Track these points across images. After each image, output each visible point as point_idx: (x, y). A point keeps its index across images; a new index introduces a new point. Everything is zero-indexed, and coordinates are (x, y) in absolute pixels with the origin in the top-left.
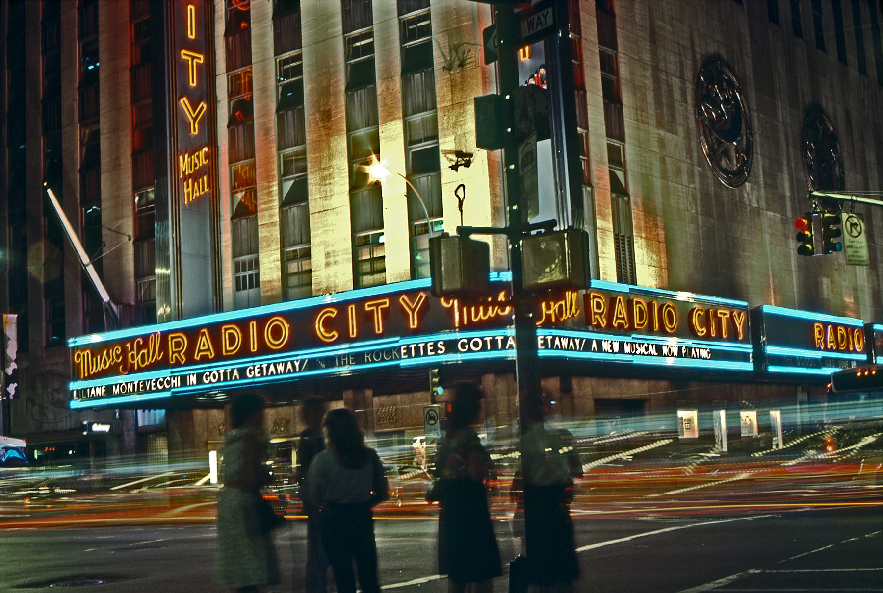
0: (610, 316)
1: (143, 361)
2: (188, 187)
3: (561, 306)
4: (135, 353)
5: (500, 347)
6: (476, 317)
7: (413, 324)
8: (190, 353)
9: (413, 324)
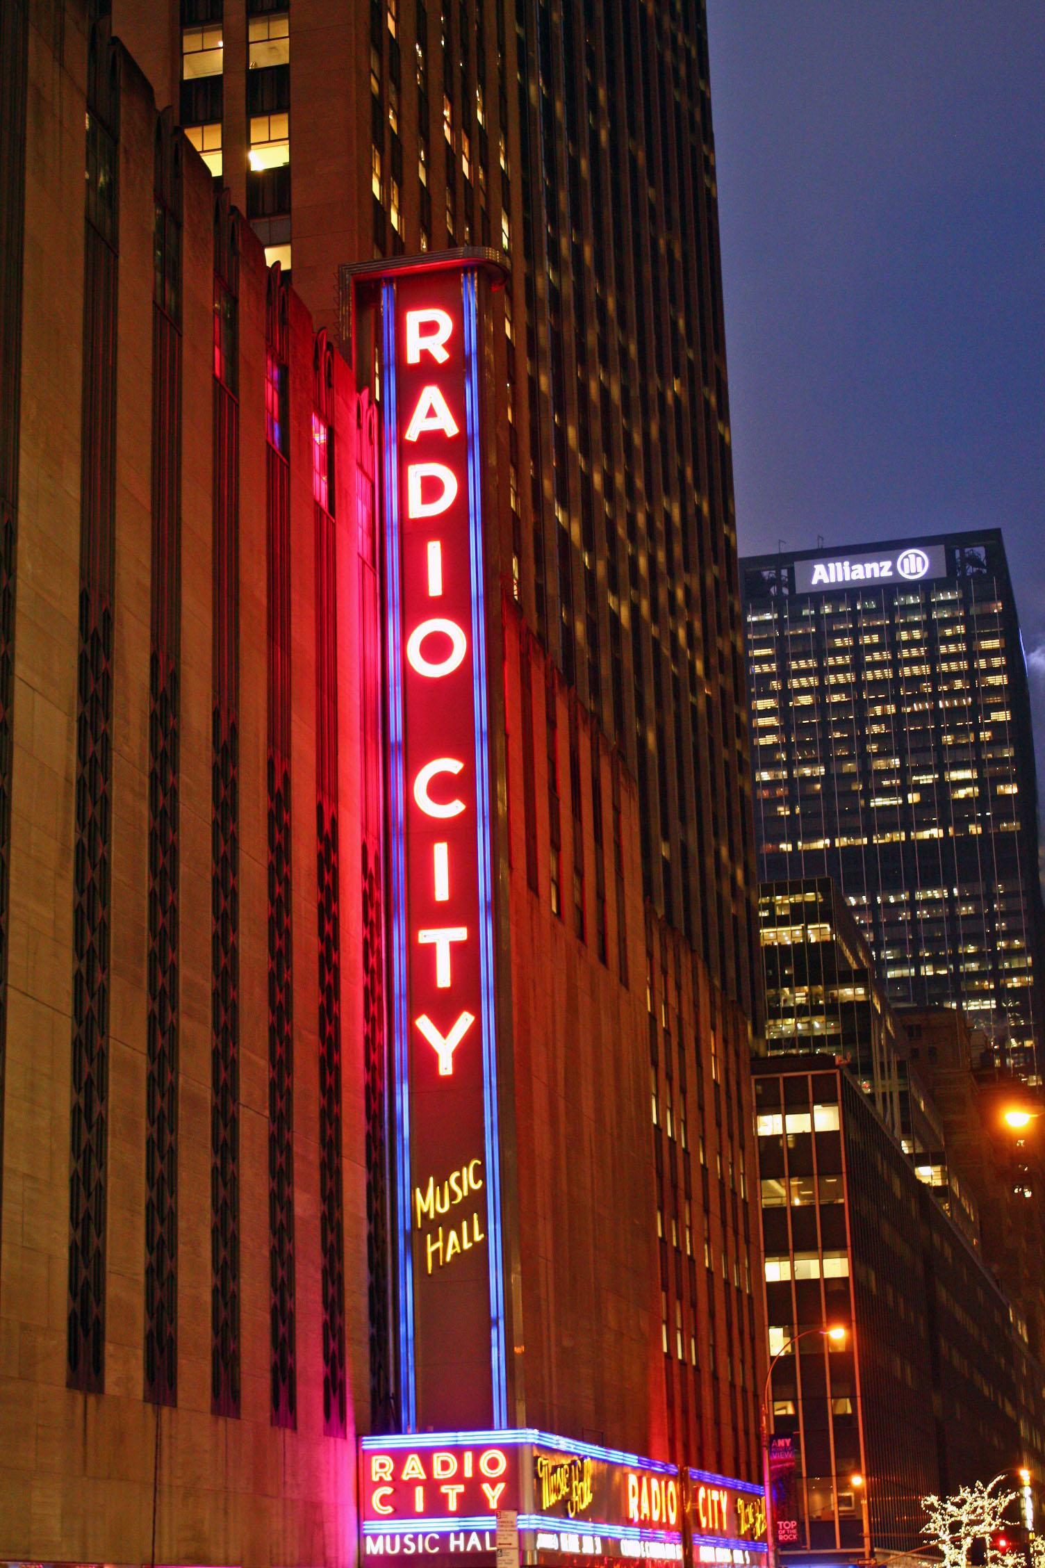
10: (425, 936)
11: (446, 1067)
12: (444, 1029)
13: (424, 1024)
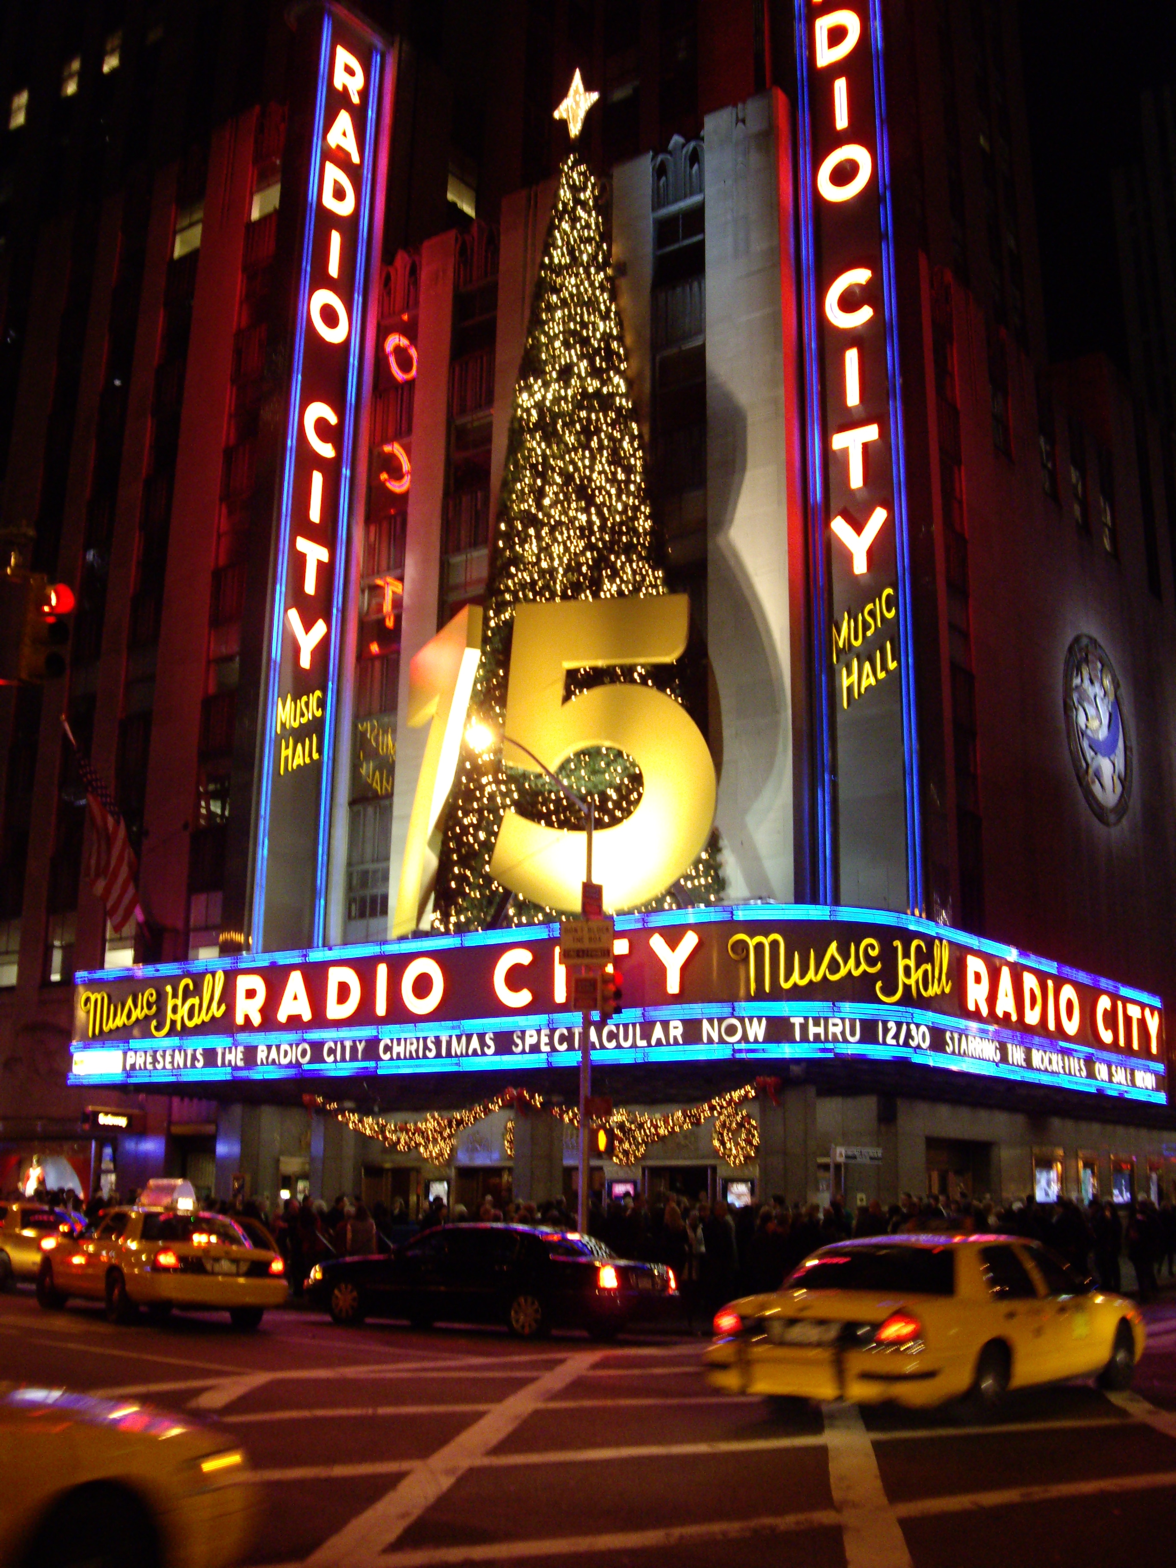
0: (992, 999)
1: (191, 1016)
2: (287, 747)
3: (926, 973)
4: (179, 1002)
5: (798, 1038)
6: (787, 979)
7: (673, 986)
8: (269, 1009)
9: (673, 986)
10: (839, 441)
11: (860, 566)
12: (858, 528)
13: (839, 526)
